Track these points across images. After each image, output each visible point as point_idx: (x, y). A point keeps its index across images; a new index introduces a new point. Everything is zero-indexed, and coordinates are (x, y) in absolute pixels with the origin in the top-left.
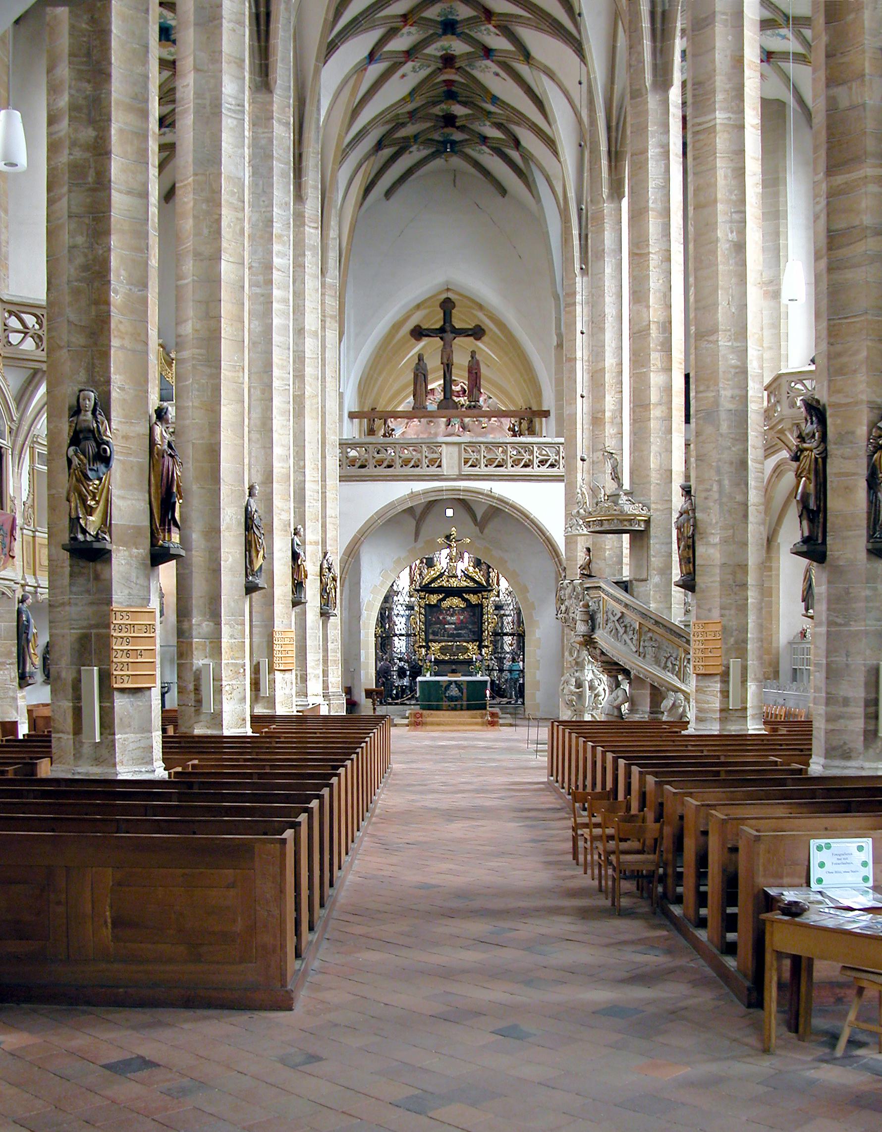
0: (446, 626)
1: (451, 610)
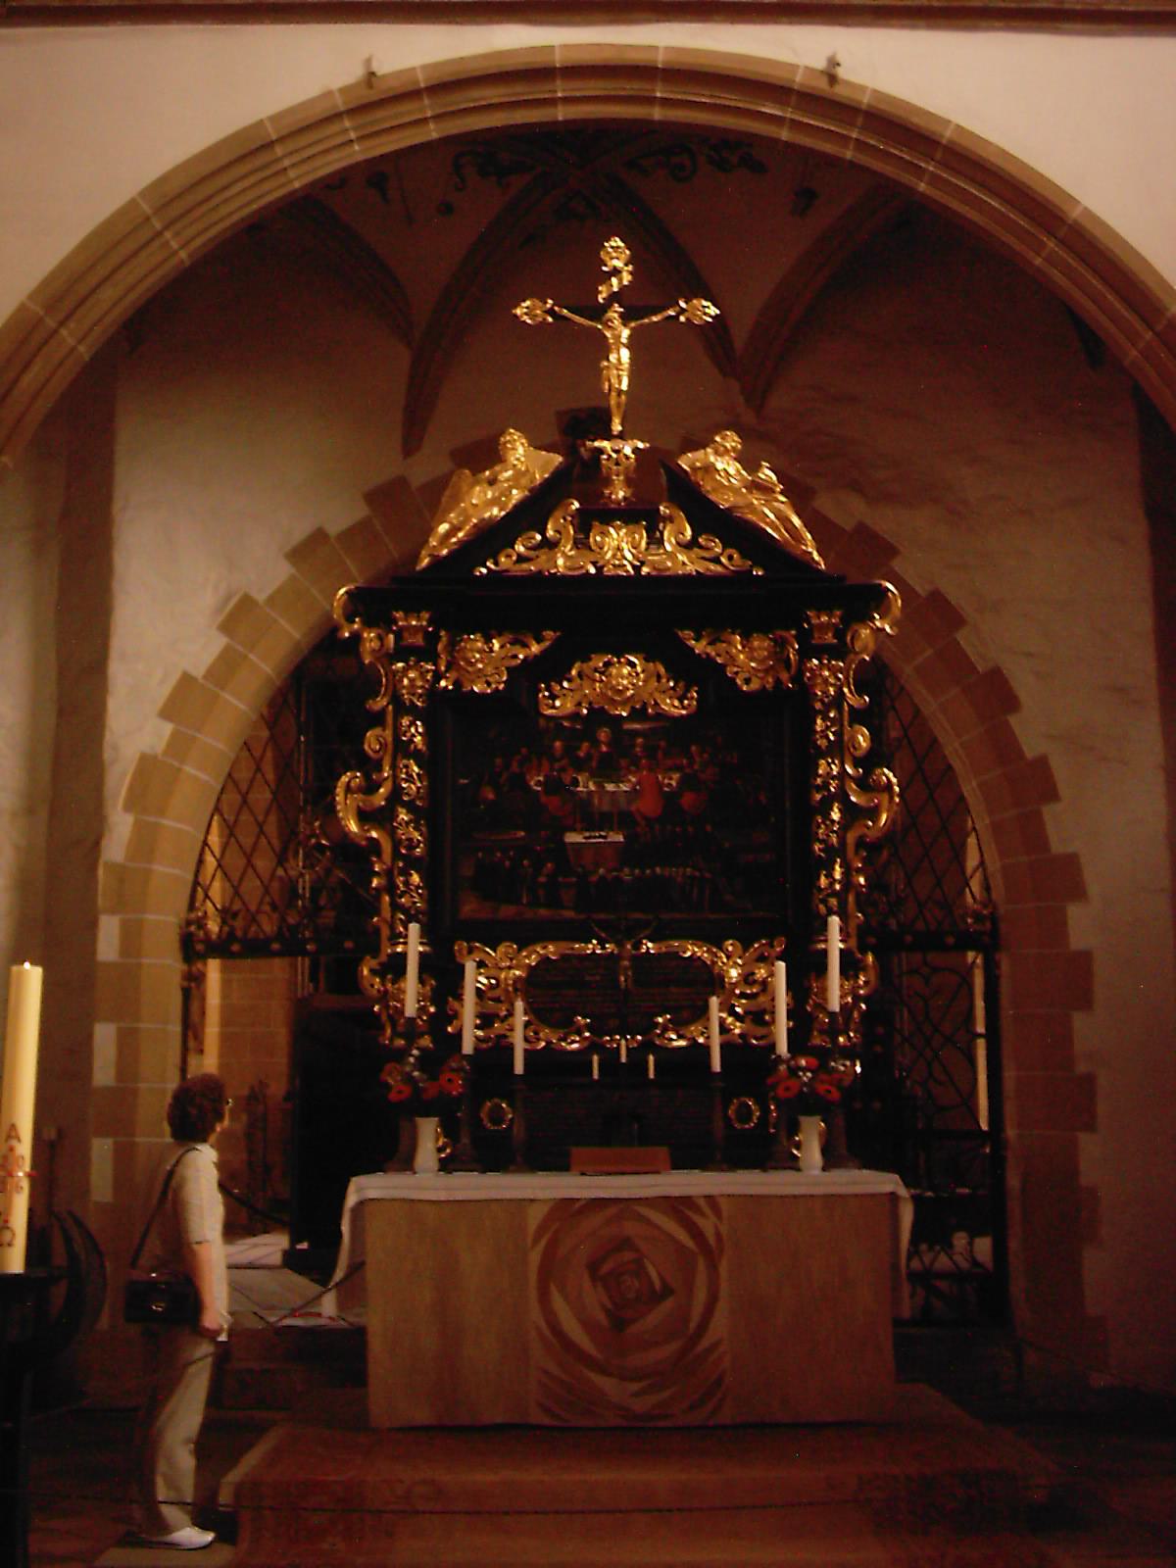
0: (573, 838)
1: (603, 734)
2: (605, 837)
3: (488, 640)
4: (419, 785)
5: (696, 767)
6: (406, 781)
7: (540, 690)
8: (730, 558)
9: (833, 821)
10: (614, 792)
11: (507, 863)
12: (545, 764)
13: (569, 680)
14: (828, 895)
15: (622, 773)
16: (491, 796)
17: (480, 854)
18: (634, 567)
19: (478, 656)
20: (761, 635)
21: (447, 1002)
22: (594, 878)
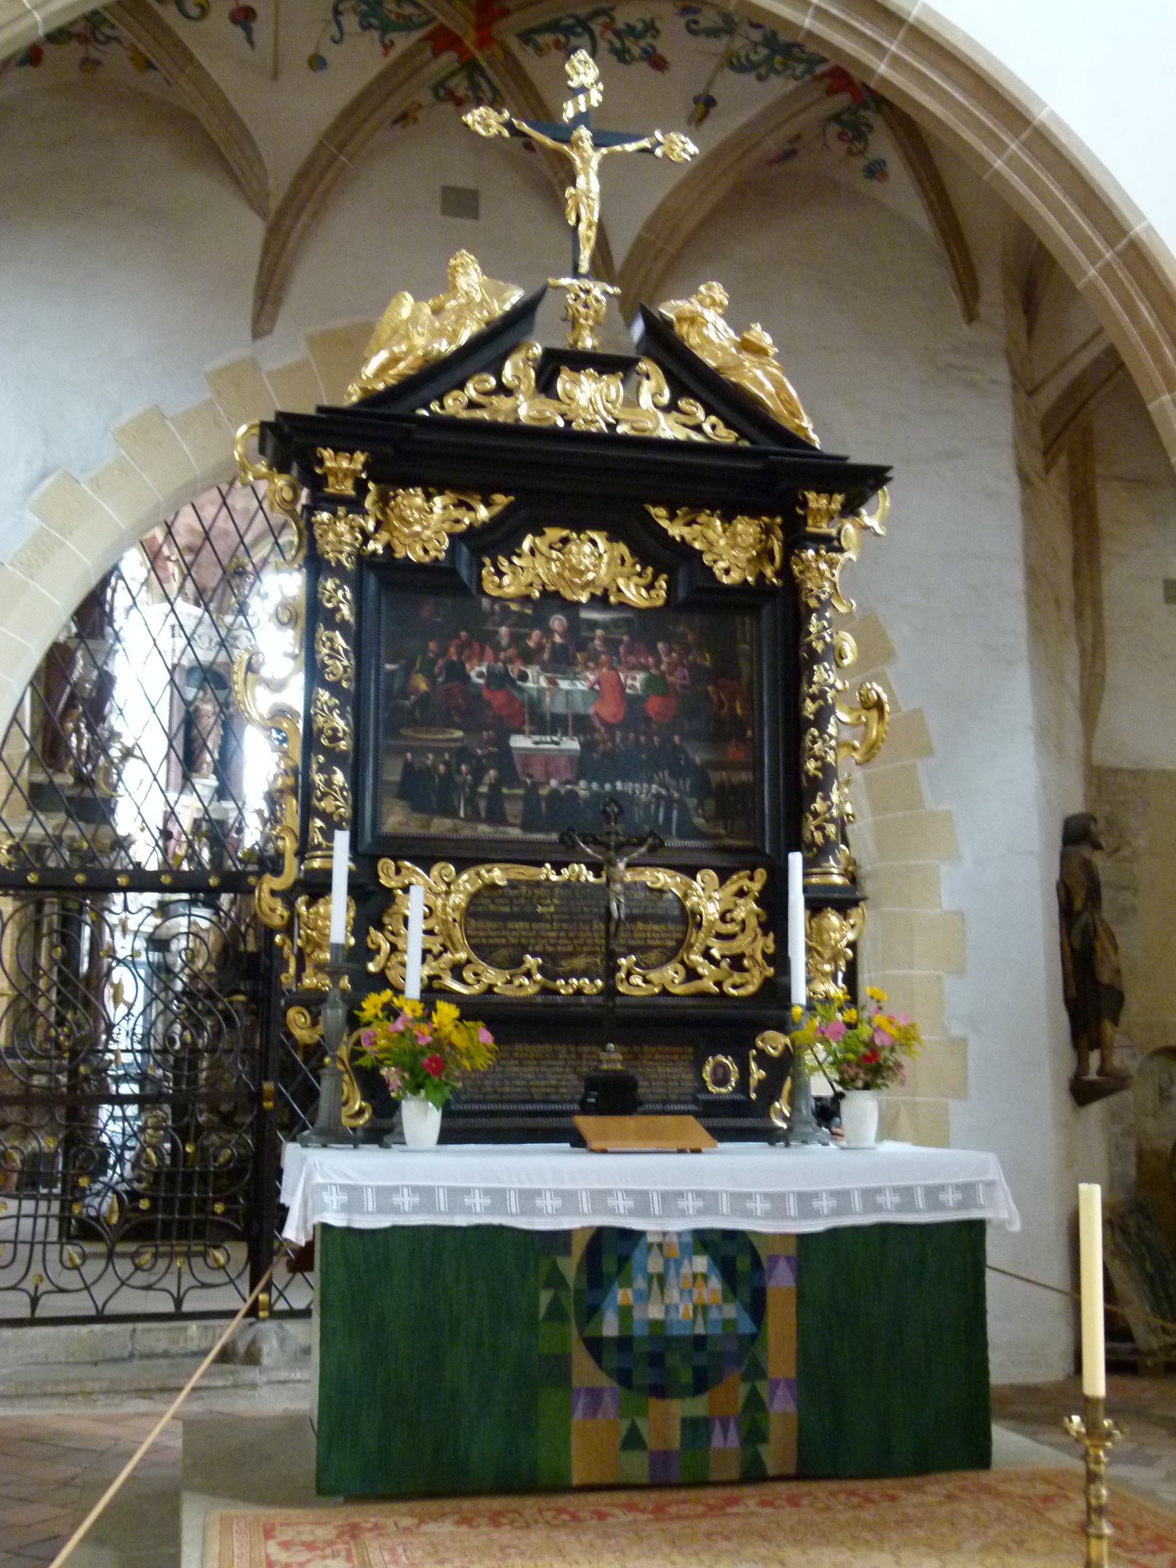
0: (519, 742)
1: (558, 622)
2: (557, 743)
3: (429, 497)
4: (346, 663)
5: (663, 667)
6: (331, 657)
7: (483, 565)
8: (714, 427)
9: (831, 737)
10: (568, 692)
11: (442, 768)
12: (489, 651)
13: (519, 556)
14: (827, 821)
15: (578, 669)
16: (423, 685)
17: (409, 755)
18: (608, 425)
19: (416, 515)
20: (746, 518)
21: (368, 933)
22: (544, 792)
